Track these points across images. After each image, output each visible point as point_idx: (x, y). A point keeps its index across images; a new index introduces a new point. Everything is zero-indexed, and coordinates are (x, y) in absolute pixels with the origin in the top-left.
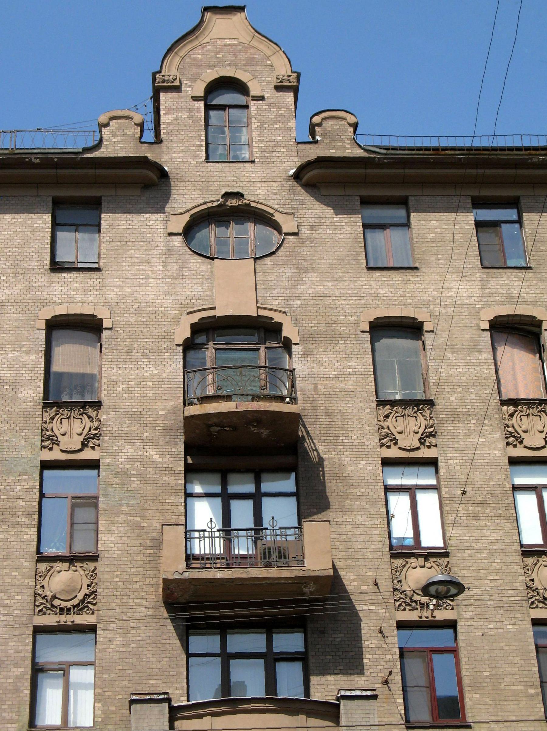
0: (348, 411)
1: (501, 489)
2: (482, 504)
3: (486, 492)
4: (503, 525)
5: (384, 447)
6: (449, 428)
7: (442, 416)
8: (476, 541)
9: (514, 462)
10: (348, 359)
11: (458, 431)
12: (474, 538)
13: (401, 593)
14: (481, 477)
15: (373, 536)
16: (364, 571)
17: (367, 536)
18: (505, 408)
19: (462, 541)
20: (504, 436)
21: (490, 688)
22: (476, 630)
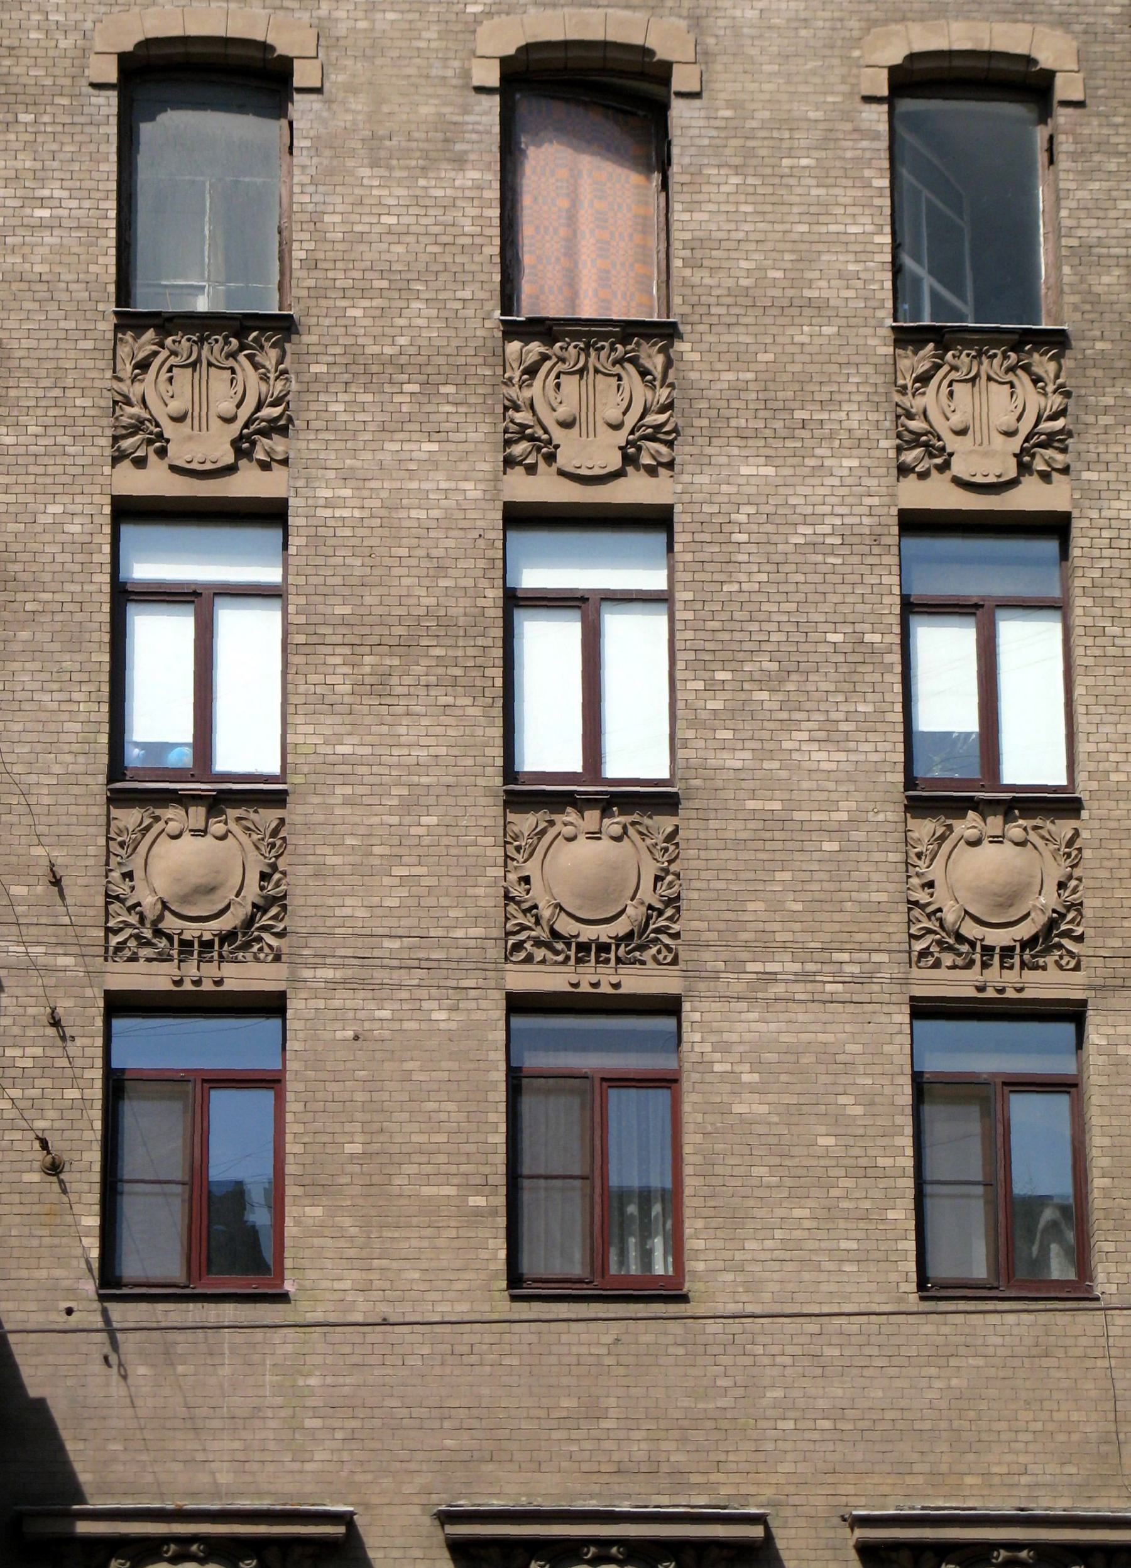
0: (25, 343)
1: (468, 602)
2: (406, 647)
3: (422, 611)
4: (458, 712)
5: (126, 464)
6: (333, 407)
7: (315, 368)
8: (371, 759)
9: (520, 517)
10: (40, 177)
11: (361, 417)
12: (368, 750)
13: (130, 909)
14: (414, 562)
15: (64, 737)
16: (24, 840)
17: (43, 737)
18: (514, 346)
19: (331, 759)
20: (500, 437)
21: (357, 1190)
22: (339, 1025)
